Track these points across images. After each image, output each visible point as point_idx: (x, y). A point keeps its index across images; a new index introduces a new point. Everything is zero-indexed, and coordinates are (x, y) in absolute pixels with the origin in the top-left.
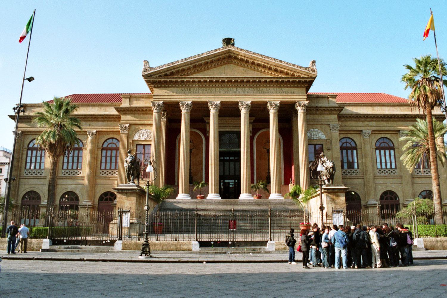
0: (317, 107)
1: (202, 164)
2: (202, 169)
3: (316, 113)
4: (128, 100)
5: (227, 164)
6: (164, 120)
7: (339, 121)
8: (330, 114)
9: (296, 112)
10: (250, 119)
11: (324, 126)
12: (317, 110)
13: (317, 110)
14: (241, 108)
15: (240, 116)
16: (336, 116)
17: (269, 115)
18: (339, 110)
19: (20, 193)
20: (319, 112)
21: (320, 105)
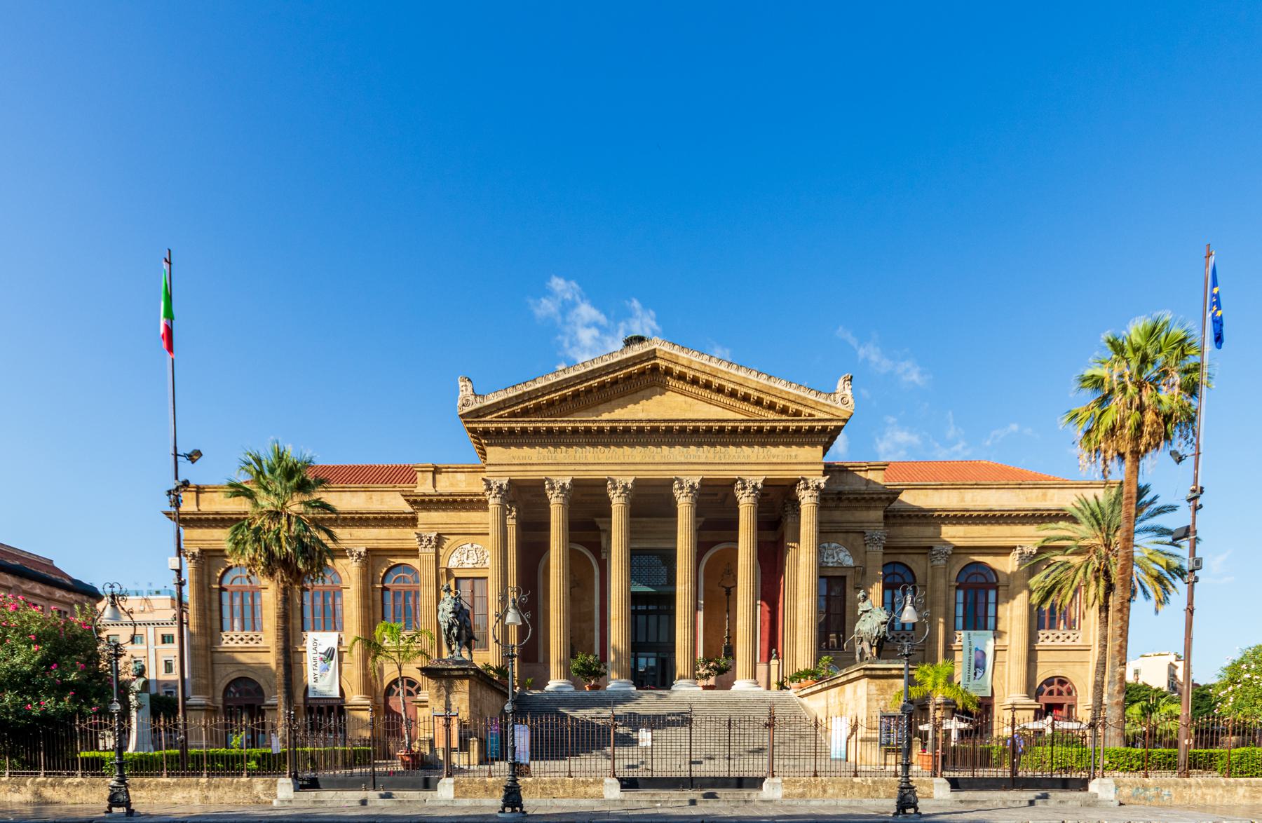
0: (843, 494)
1: (592, 619)
2: (592, 630)
3: (837, 508)
4: (430, 475)
5: (642, 619)
6: (511, 522)
7: (886, 525)
8: (868, 508)
9: (796, 503)
10: (697, 522)
11: (851, 537)
12: (840, 499)
13: (840, 499)
14: (677, 493)
15: (673, 513)
16: (881, 513)
17: (738, 510)
18: (888, 499)
19: (217, 681)
20: (845, 504)
21: (847, 488)
